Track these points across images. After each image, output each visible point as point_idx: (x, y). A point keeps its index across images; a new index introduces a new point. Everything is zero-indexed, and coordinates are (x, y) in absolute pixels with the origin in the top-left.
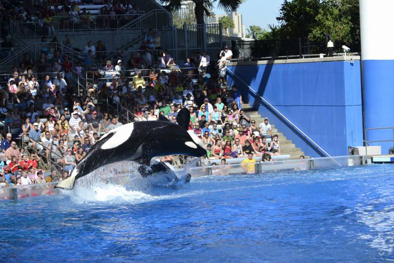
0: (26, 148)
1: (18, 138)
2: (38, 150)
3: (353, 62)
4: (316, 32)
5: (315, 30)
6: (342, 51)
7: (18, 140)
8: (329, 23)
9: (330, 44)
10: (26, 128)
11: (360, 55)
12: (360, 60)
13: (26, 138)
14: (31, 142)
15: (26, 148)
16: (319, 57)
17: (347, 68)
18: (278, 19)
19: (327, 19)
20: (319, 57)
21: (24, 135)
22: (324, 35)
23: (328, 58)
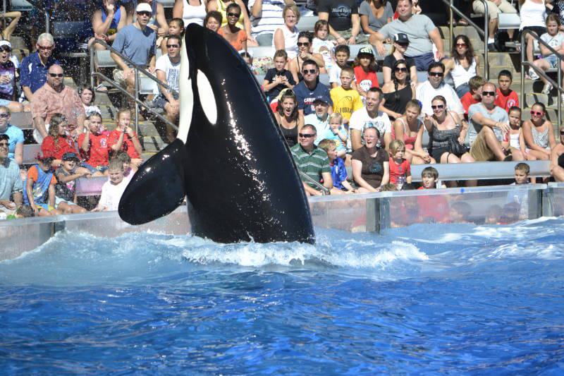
0: (102, 87)
1: (76, 55)
2: (142, 98)
7: (79, 58)
10: (103, 20)
13: (103, 56)
14: (120, 68)
15: (102, 87)
21: (99, 45)
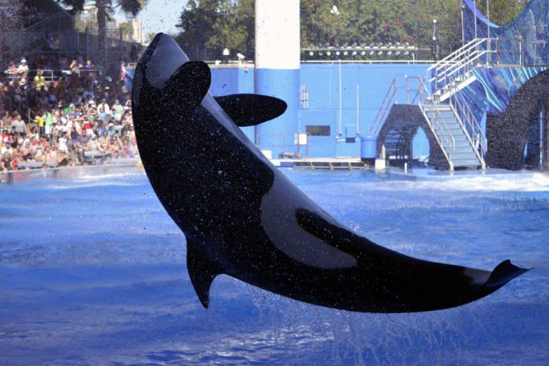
3: (247, 70)
4: (213, 40)
5: (212, 38)
6: (237, 59)
8: (225, 32)
9: (226, 52)
11: (254, 63)
12: (255, 68)
16: (214, 63)
17: (241, 74)
18: (177, 26)
19: (224, 28)
20: (214, 63)
22: (221, 43)
23: (223, 66)
